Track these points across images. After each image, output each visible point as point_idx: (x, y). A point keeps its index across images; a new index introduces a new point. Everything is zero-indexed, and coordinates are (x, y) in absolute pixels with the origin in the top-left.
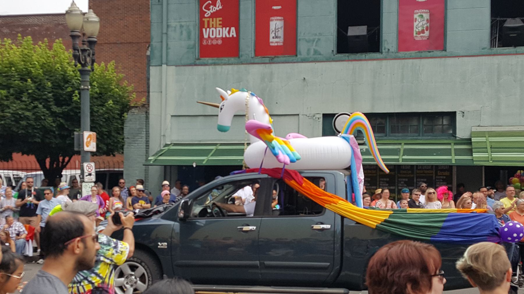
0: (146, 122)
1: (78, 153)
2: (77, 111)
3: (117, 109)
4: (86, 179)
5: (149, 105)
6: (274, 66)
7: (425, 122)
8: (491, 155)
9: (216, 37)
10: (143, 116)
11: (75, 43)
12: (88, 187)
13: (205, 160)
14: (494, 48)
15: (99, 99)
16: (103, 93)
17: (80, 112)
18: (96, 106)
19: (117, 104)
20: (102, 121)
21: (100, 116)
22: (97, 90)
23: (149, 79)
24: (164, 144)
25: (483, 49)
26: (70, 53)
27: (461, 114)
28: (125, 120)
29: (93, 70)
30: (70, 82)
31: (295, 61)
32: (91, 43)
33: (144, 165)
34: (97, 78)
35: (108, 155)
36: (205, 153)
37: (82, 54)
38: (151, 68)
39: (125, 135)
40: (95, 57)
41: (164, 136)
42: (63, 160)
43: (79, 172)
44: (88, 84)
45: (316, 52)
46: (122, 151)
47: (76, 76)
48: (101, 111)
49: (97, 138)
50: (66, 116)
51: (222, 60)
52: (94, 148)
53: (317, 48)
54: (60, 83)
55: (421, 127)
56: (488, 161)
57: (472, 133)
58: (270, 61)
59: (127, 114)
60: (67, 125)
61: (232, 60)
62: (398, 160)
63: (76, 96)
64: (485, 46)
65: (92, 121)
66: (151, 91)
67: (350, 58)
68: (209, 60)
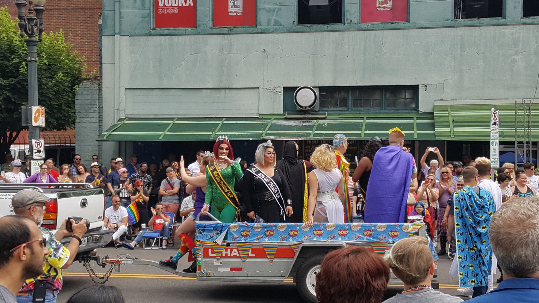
0: (99, 95)
1: (27, 128)
2: (25, 84)
3: (68, 81)
4: (35, 156)
5: (102, 77)
6: (233, 37)
7: (388, 95)
8: (453, 129)
9: (172, 6)
10: (95, 88)
11: (20, 12)
12: (38, 164)
13: (161, 135)
14: (458, 20)
15: (48, 71)
16: (52, 64)
17: (27, 85)
18: (45, 79)
19: (68, 77)
20: (51, 94)
21: (49, 88)
22: (46, 61)
23: (101, 50)
24: (119, 118)
25: (446, 21)
26: (16, 21)
27: (424, 88)
28: (76, 93)
29: (40, 40)
30: (18, 53)
31: (255, 32)
32: (39, 12)
33: (96, 141)
34: (45, 48)
35: (59, 130)
36: (162, 128)
37: (29, 24)
38: (103, 37)
39: (76, 108)
40: (43, 27)
41: (118, 109)
42: (11, 135)
43: (27, 147)
44: (36, 55)
45: (276, 22)
46: (73, 125)
47: (23, 47)
48: (51, 84)
49: (46, 112)
50: (13, 89)
51: (179, 30)
52: (43, 123)
53: (277, 18)
54: (6, 54)
55: (384, 100)
56: (450, 136)
57: (434, 106)
58: (229, 31)
59: (79, 87)
60: (15, 99)
61: (190, 30)
62: (359, 135)
63: (23, 67)
64: (449, 17)
65: (41, 94)
66: (104, 61)
67: (311, 28)
68: (165, 30)
